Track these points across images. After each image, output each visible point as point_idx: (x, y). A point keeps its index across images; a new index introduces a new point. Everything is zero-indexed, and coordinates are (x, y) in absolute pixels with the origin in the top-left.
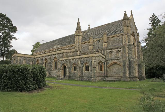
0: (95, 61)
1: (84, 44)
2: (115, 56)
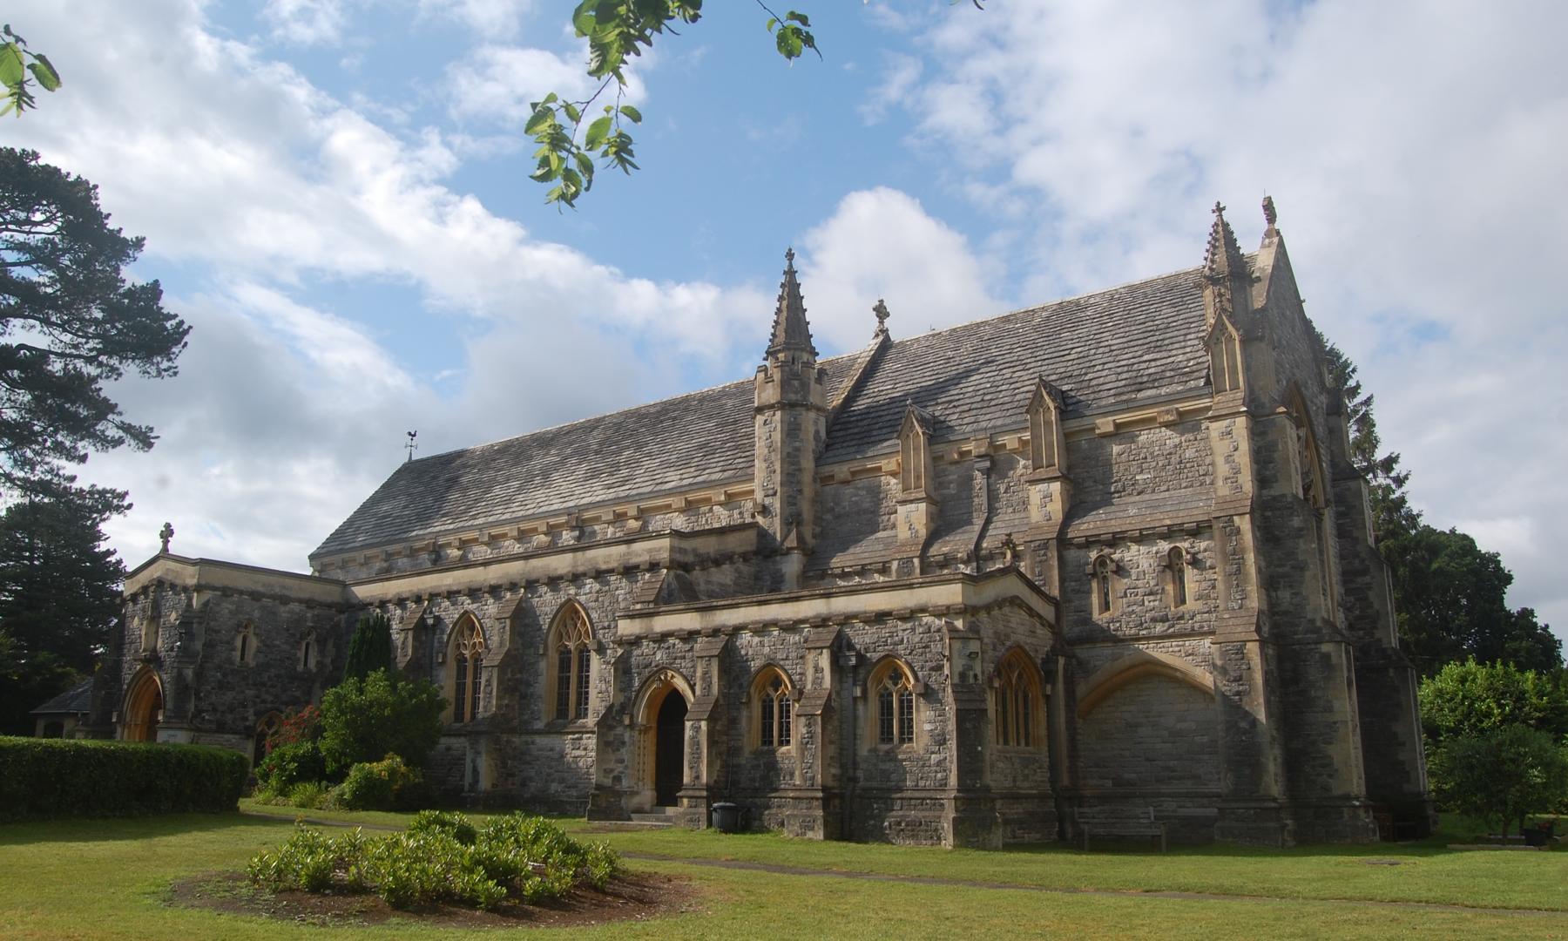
1: (846, 482)
2: (1150, 603)
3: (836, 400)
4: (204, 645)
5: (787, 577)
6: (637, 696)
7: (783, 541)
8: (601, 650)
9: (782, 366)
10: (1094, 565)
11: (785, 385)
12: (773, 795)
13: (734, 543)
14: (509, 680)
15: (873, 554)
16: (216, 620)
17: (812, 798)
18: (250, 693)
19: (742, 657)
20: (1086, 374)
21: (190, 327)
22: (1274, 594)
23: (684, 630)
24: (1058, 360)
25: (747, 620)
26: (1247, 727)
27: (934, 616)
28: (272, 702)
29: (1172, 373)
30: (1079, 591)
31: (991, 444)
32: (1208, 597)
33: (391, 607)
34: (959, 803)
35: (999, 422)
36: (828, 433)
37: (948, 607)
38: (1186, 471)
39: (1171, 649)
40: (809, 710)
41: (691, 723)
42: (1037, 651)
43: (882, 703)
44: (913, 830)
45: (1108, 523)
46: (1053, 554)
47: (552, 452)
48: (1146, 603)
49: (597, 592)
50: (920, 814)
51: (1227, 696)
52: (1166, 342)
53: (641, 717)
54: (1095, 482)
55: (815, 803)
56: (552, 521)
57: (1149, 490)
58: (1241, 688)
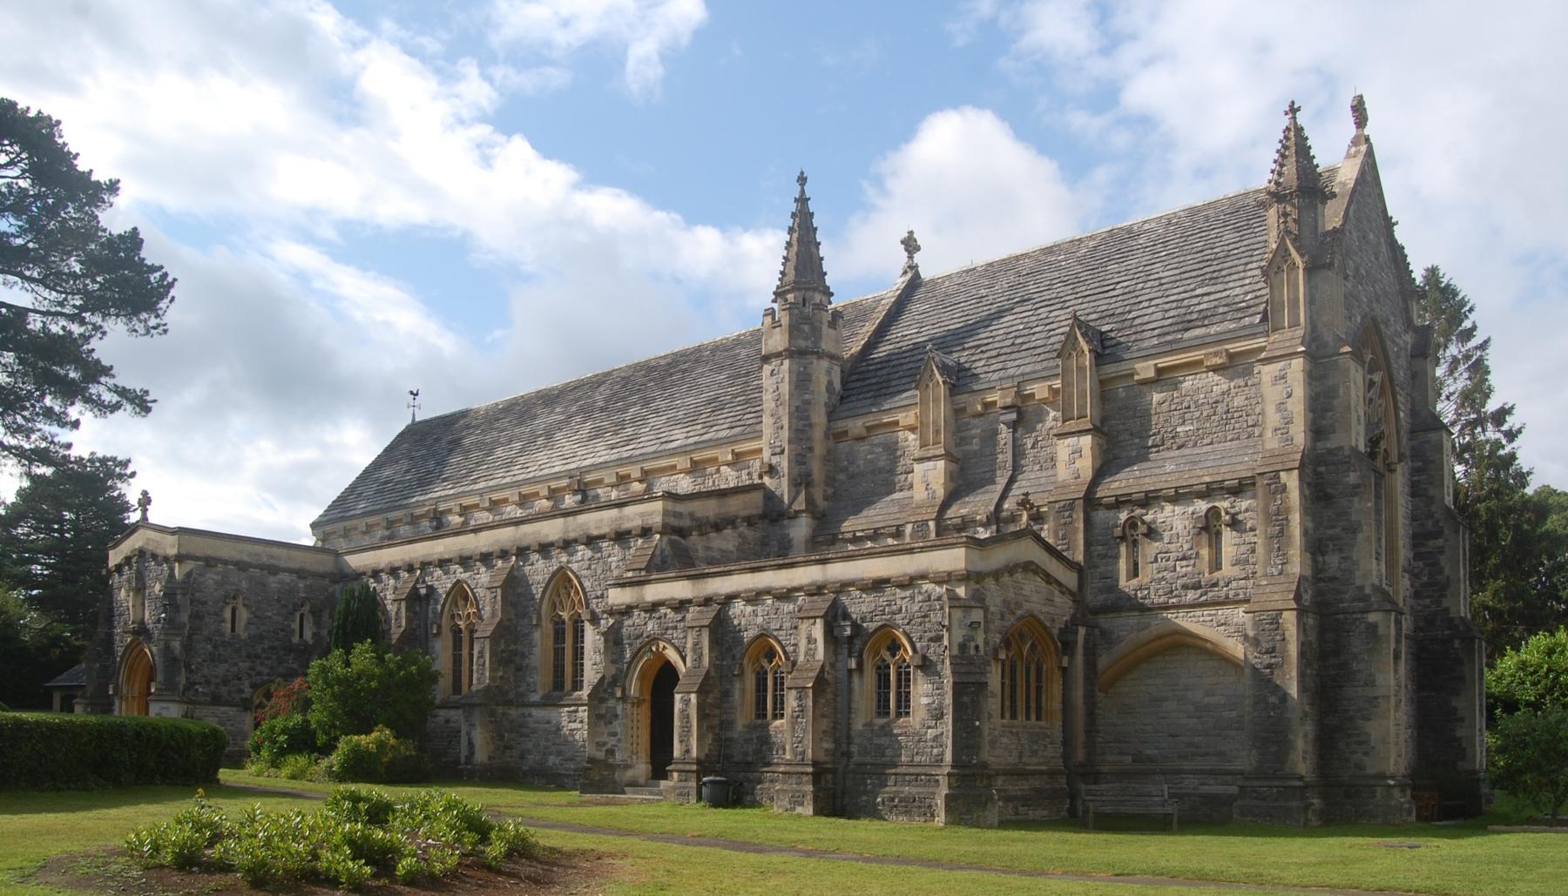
0: (973, 626)
1: (860, 439)
3: (855, 347)
4: (190, 617)
5: (795, 542)
6: (628, 668)
7: (792, 501)
8: (595, 620)
9: (791, 308)
10: (1124, 527)
11: (794, 330)
13: (735, 505)
14: (503, 651)
15: (886, 517)
16: (200, 591)
19: (735, 627)
22: (1321, 559)
23: (675, 599)
25: (740, 589)
27: (935, 583)
30: (1105, 556)
31: (1018, 393)
33: (384, 576)
35: (1028, 369)
36: (844, 383)
37: (949, 574)
39: (1201, 619)
40: (800, 683)
41: (680, 695)
42: (1054, 620)
43: (880, 675)
46: (1079, 516)
47: (558, 410)
48: (1178, 569)
49: (590, 559)
53: (633, 690)
56: (554, 485)
58: (1273, 660)
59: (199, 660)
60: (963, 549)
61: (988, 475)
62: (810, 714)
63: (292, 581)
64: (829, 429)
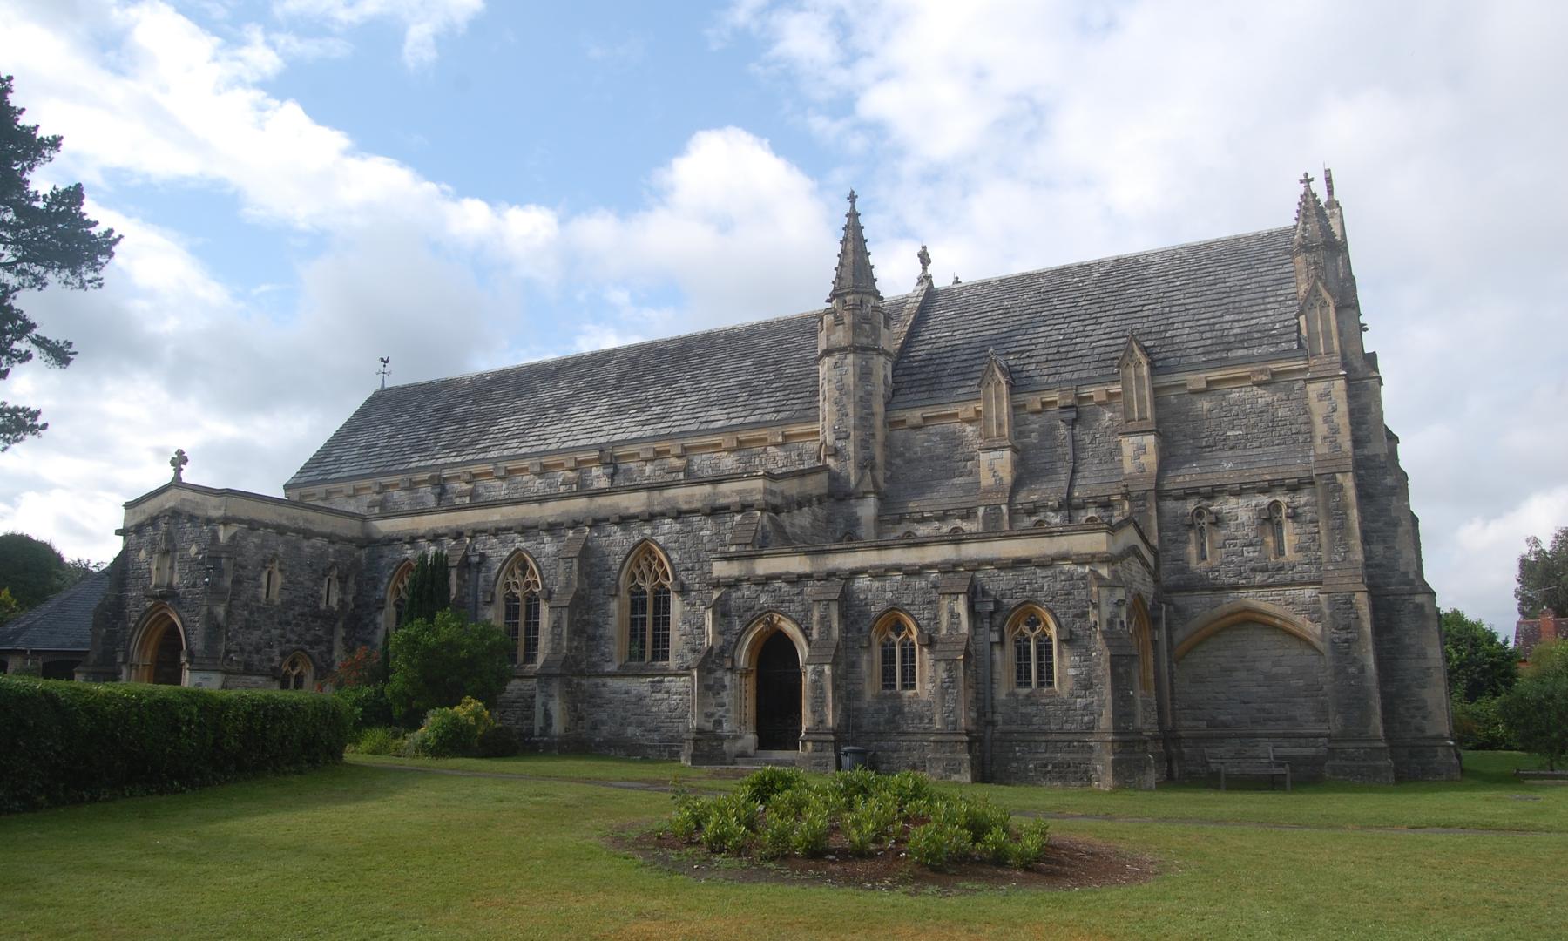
2: (1249, 553)
4: (233, 582)
5: (863, 521)
6: (738, 640)
7: (857, 485)
10: (1192, 515)
11: (856, 328)
12: (902, 738)
14: (578, 620)
15: (953, 500)
17: (956, 742)
18: (276, 632)
20: (1166, 331)
21: (121, 237)
22: (1368, 547)
23: (793, 574)
24: (1130, 315)
25: (865, 564)
26: (1356, 672)
28: (297, 642)
29: (1260, 335)
32: (1308, 549)
34: (1116, 746)
37: (1093, 556)
38: (1278, 429)
39: (1271, 598)
40: (949, 655)
41: (812, 666)
44: (1060, 772)
45: (1204, 476)
47: (561, 385)
48: (1246, 554)
50: (1068, 757)
51: (1336, 643)
52: (1245, 304)
53: (743, 659)
54: (1185, 436)
55: (960, 747)
56: (581, 456)
57: (1241, 446)
58: (1350, 636)
59: (236, 627)
60: (1105, 534)
61: (1048, 466)
62: (962, 685)
63: (324, 545)
64: (886, 417)
